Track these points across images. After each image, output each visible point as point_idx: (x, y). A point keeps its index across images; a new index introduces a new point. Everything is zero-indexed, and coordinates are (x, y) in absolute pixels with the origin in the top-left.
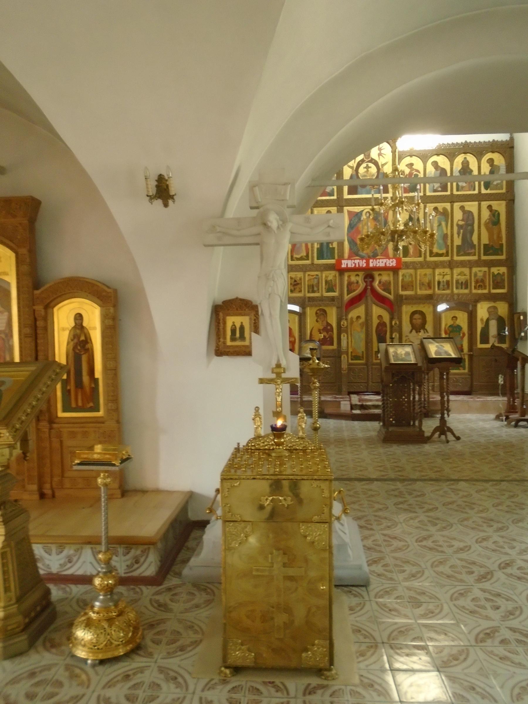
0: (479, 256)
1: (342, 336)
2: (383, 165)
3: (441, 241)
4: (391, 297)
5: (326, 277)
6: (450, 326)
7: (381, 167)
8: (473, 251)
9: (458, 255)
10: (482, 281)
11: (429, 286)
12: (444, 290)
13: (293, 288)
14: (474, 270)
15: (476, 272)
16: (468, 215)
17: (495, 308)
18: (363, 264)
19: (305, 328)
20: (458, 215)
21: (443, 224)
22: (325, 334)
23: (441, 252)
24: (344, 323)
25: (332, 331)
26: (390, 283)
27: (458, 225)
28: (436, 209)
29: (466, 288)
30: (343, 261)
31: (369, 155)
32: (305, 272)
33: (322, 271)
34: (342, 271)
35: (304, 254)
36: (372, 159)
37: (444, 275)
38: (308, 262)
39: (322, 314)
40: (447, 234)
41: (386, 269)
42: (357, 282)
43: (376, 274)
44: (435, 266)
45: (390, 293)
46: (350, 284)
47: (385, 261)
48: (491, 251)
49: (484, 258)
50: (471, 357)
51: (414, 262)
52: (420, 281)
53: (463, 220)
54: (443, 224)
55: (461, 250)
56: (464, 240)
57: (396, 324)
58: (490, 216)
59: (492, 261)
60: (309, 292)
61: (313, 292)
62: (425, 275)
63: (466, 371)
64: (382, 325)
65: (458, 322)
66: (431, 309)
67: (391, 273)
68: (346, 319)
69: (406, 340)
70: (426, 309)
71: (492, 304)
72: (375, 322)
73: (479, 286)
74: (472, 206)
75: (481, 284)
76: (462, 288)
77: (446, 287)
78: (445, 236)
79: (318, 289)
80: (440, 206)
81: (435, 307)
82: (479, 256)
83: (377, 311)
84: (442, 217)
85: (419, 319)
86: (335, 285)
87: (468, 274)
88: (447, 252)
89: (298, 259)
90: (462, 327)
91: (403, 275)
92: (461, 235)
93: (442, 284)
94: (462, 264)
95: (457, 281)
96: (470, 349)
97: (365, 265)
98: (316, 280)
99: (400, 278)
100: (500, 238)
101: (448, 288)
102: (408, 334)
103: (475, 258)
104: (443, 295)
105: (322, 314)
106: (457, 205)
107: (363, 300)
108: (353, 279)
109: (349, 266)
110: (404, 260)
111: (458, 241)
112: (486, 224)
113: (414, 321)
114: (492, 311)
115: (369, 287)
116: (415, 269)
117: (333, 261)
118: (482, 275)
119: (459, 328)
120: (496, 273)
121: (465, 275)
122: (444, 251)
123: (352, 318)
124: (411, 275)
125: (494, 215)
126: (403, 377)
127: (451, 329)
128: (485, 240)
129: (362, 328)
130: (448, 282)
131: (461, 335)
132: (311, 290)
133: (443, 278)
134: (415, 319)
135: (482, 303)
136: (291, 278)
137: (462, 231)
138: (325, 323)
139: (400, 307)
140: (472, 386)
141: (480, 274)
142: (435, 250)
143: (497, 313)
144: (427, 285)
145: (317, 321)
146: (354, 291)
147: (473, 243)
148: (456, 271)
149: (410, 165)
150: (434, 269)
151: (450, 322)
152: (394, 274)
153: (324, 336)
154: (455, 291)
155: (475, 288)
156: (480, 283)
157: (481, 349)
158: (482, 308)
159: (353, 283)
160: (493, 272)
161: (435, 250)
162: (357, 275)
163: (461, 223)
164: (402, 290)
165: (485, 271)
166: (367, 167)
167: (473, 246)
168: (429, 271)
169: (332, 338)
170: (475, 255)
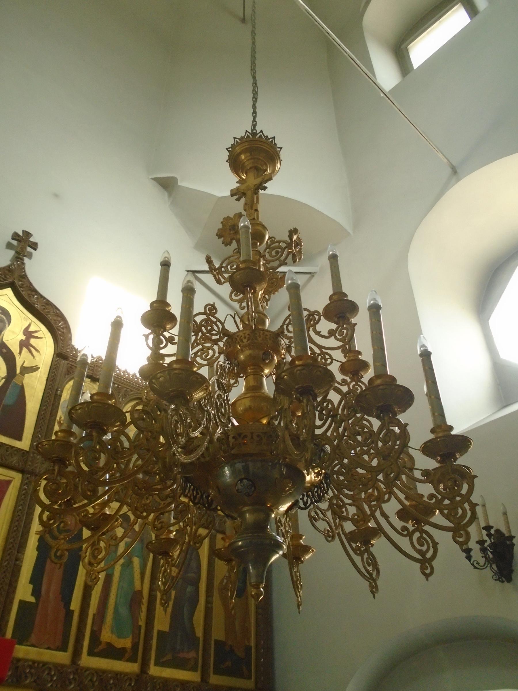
2: (26, 370)
3: (124, 611)
7: (18, 371)
8: (192, 655)
21: (136, 561)
40: (140, 592)
48: (228, 663)
51: (45, 664)
54: (136, 561)
88: (135, 646)
92: (171, 603)
112: (223, 589)
122: (127, 643)
161: (106, 635)
167: (193, 641)
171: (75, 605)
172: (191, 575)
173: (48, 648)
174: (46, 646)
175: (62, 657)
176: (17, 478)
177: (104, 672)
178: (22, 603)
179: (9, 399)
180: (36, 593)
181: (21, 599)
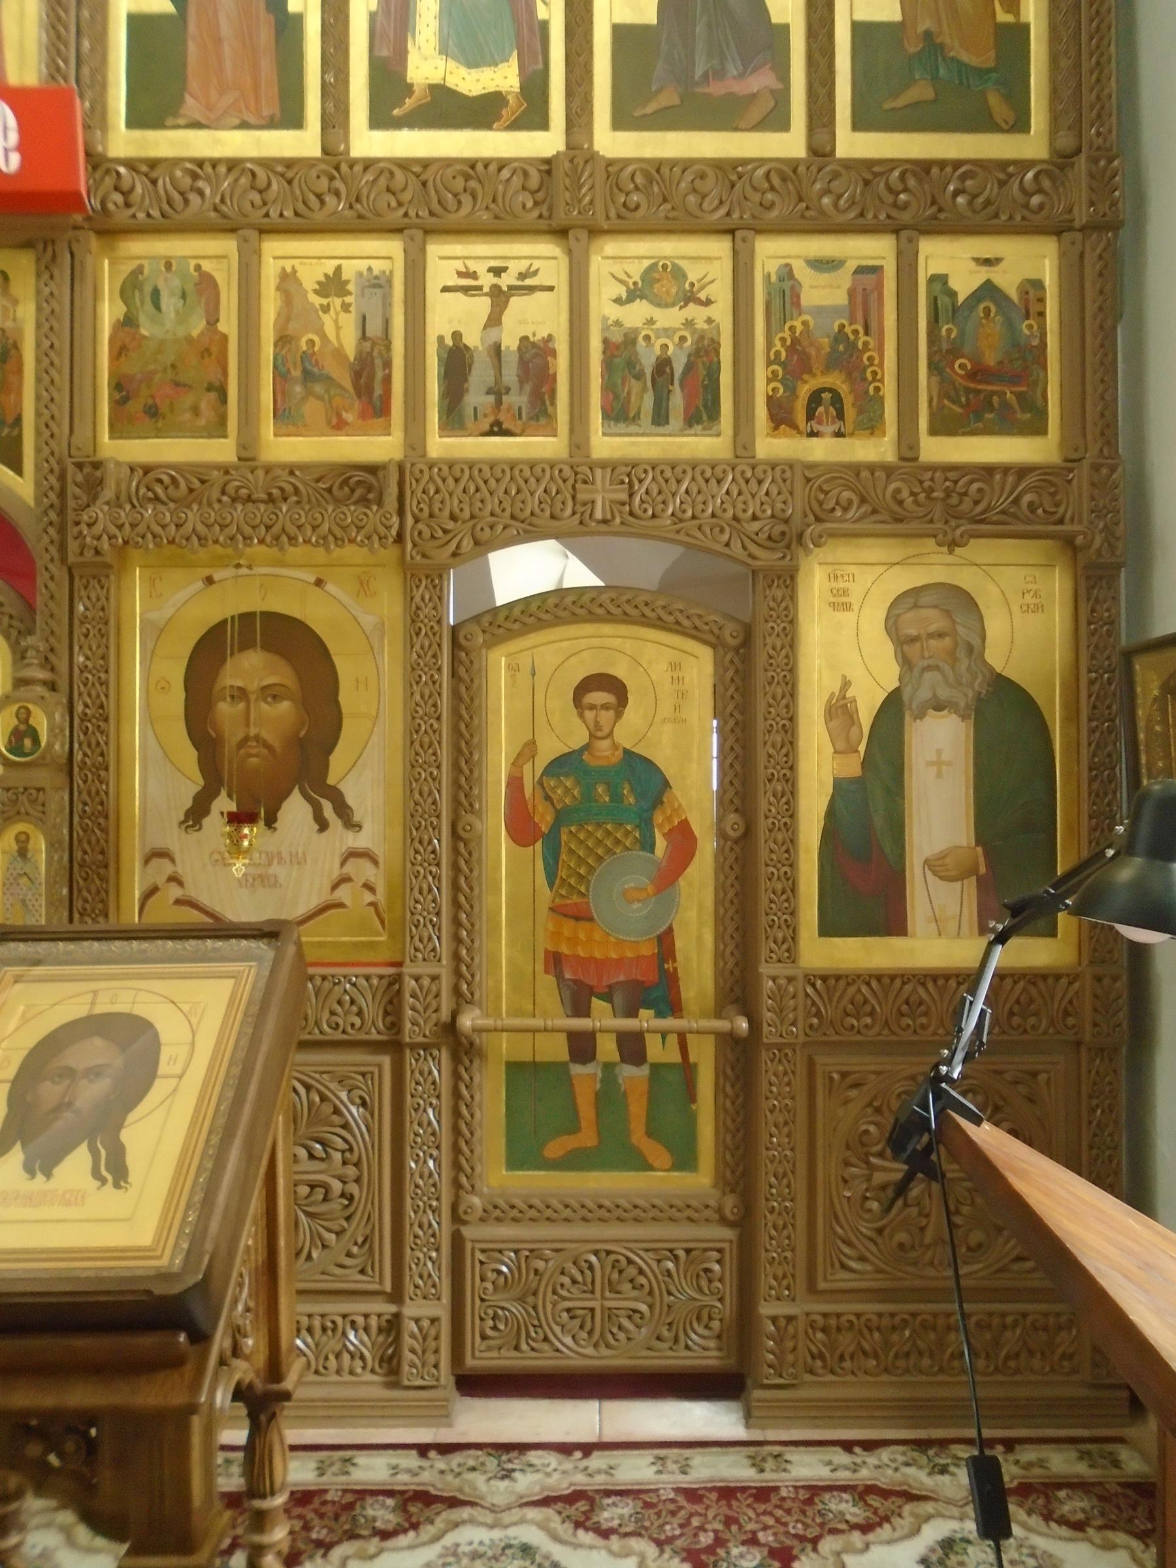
6: (562, 764)
8: (761, 81)
9: (621, 122)
10: (848, 355)
11: (366, 388)
12: (498, 429)
14: (772, 252)
15: (787, 273)
17: (960, 602)
23: (472, 82)
29: (703, 412)
37: (500, 298)
50: (740, 1057)
52: (283, 340)
62: (333, 285)
63: (700, 1181)
65: (630, 730)
66: (387, 604)
69: (150, 893)
71: (935, 567)
73: (815, 399)
75: (835, 380)
76: (660, 417)
77: (517, 399)
81: (422, 579)
85: (272, 694)
87: (721, 292)
90: (670, 772)
91: (130, 287)
96: (738, 990)
99: (109, 312)
101: (539, 413)
113: (225, 710)
114: (934, 629)
118: (840, 298)
119: (644, 780)
120: (964, 284)
121: (690, 298)
122: (505, 77)
127: (566, 790)
130: (535, 358)
133: (494, 320)
134: (241, 694)
135: (840, 552)
140: (743, 1328)
141: (824, 294)
142: (426, 65)
143: (975, 651)
144: (347, 383)
151: (565, 733)
152: (46, 269)
155: (780, 417)
156: (823, 379)
157: (832, 981)
158: (840, 603)
160: (939, 281)
161: (426, 65)
164: (115, 433)
165: (877, 270)
170: (778, 120)
173: (244, 125)
174: (237, 122)
177: (426, 163)
181: (135, 8)
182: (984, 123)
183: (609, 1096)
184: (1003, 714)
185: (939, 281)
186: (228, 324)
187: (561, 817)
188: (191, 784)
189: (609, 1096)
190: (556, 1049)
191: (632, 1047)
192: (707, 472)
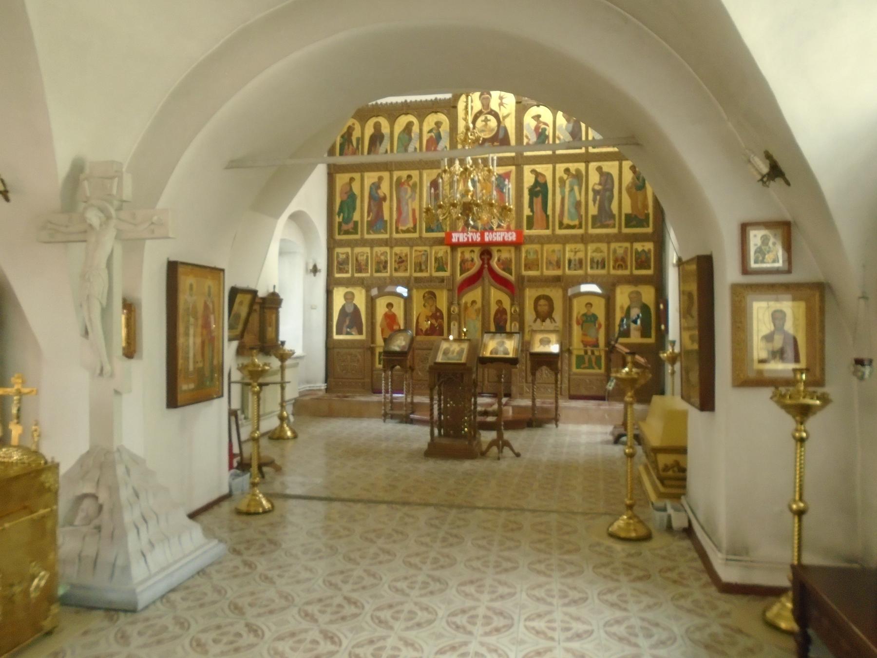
0: (620, 228)
1: (452, 324)
2: (504, 118)
3: (573, 210)
4: (512, 278)
5: (436, 253)
6: (584, 315)
8: (611, 222)
9: (593, 227)
10: (623, 260)
11: (558, 265)
13: (397, 266)
14: (613, 245)
16: (606, 178)
17: (638, 294)
18: (477, 238)
19: (411, 315)
20: (594, 178)
21: (576, 188)
22: (434, 321)
23: (572, 223)
24: (455, 309)
25: (442, 318)
26: (511, 261)
27: (594, 190)
28: (567, 171)
29: (603, 267)
30: (454, 235)
31: (488, 105)
32: (411, 247)
33: (431, 246)
34: (454, 247)
35: (410, 225)
36: (492, 110)
37: (576, 252)
38: (416, 235)
39: (431, 296)
41: (504, 244)
42: (472, 260)
43: (494, 250)
44: (565, 240)
45: (511, 274)
46: (463, 262)
47: (502, 234)
48: (634, 223)
49: (625, 230)
53: (600, 184)
54: (576, 188)
55: (597, 221)
56: (601, 208)
57: (515, 311)
58: (633, 178)
59: (634, 234)
60: (415, 271)
61: (421, 271)
63: (602, 371)
64: (501, 312)
67: (513, 249)
68: (459, 304)
70: (556, 294)
72: (494, 308)
74: (611, 167)
77: (578, 266)
78: (578, 204)
79: (427, 268)
80: (573, 167)
81: (565, 291)
82: (620, 228)
83: (496, 294)
84: (575, 181)
86: (447, 264)
89: (404, 232)
91: (527, 252)
92: (597, 202)
93: (573, 262)
94: (599, 239)
95: (592, 260)
97: (479, 239)
98: (424, 258)
99: (523, 255)
100: (645, 206)
101: (581, 267)
102: (532, 323)
103: (615, 231)
104: (574, 276)
105: (431, 296)
106: (593, 165)
107: (480, 281)
108: (468, 256)
109: (461, 240)
110: (527, 232)
111: (593, 210)
113: (539, 308)
114: (635, 297)
115: (486, 266)
116: (542, 244)
117: (442, 235)
119: (594, 318)
121: (601, 252)
122: (576, 222)
123: (466, 303)
124: (536, 252)
125: (638, 178)
126: (452, 380)
127: (585, 318)
128: (627, 209)
129: (478, 315)
130: (581, 261)
131: (597, 326)
132: (418, 269)
136: (396, 254)
137: (598, 197)
138: (434, 309)
139: (522, 290)
141: (620, 252)
142: (566, 221)
143: (640, 300)
145: (424, 306)
146: (468, 270)
147: (611, 211)
148: (591, 247)
149: (537, 117)
150: (564, 244)
151: (584, 311)
153: (431, 324)
154: (590, 271)
155: (614, 268)
156: (620, 263)
159: (467, 260)
161: (566, 221)
162: (472, 251)
163: (598, 187)
165: (627, 248)
166: (486, 120)
167: (612, 216)
168: (557, 247)
169: (441, 327)
170: (614, 226)
171: (550, 212)
172: (608, 186)
175: (548, 232)
176: (513, 168)
178: (528, 217)
179: (501, 135)
180: (532, 211)
182: (643, 226)
183: (590, 360)
184: (645, 308)
185: (636, 250)
186: (540, 256)
187: (584, 322)
188: (535, 316)
189: (590, 360)
190: (582, 353)
191: (593, 353)
192: (603, 276)
